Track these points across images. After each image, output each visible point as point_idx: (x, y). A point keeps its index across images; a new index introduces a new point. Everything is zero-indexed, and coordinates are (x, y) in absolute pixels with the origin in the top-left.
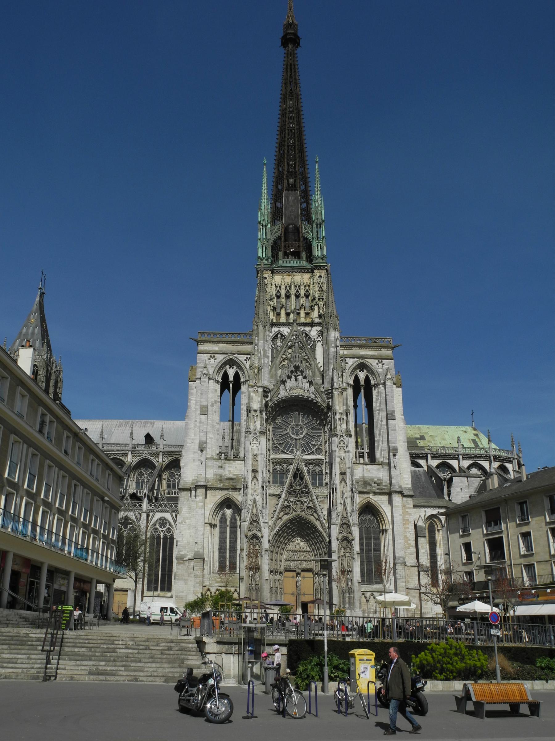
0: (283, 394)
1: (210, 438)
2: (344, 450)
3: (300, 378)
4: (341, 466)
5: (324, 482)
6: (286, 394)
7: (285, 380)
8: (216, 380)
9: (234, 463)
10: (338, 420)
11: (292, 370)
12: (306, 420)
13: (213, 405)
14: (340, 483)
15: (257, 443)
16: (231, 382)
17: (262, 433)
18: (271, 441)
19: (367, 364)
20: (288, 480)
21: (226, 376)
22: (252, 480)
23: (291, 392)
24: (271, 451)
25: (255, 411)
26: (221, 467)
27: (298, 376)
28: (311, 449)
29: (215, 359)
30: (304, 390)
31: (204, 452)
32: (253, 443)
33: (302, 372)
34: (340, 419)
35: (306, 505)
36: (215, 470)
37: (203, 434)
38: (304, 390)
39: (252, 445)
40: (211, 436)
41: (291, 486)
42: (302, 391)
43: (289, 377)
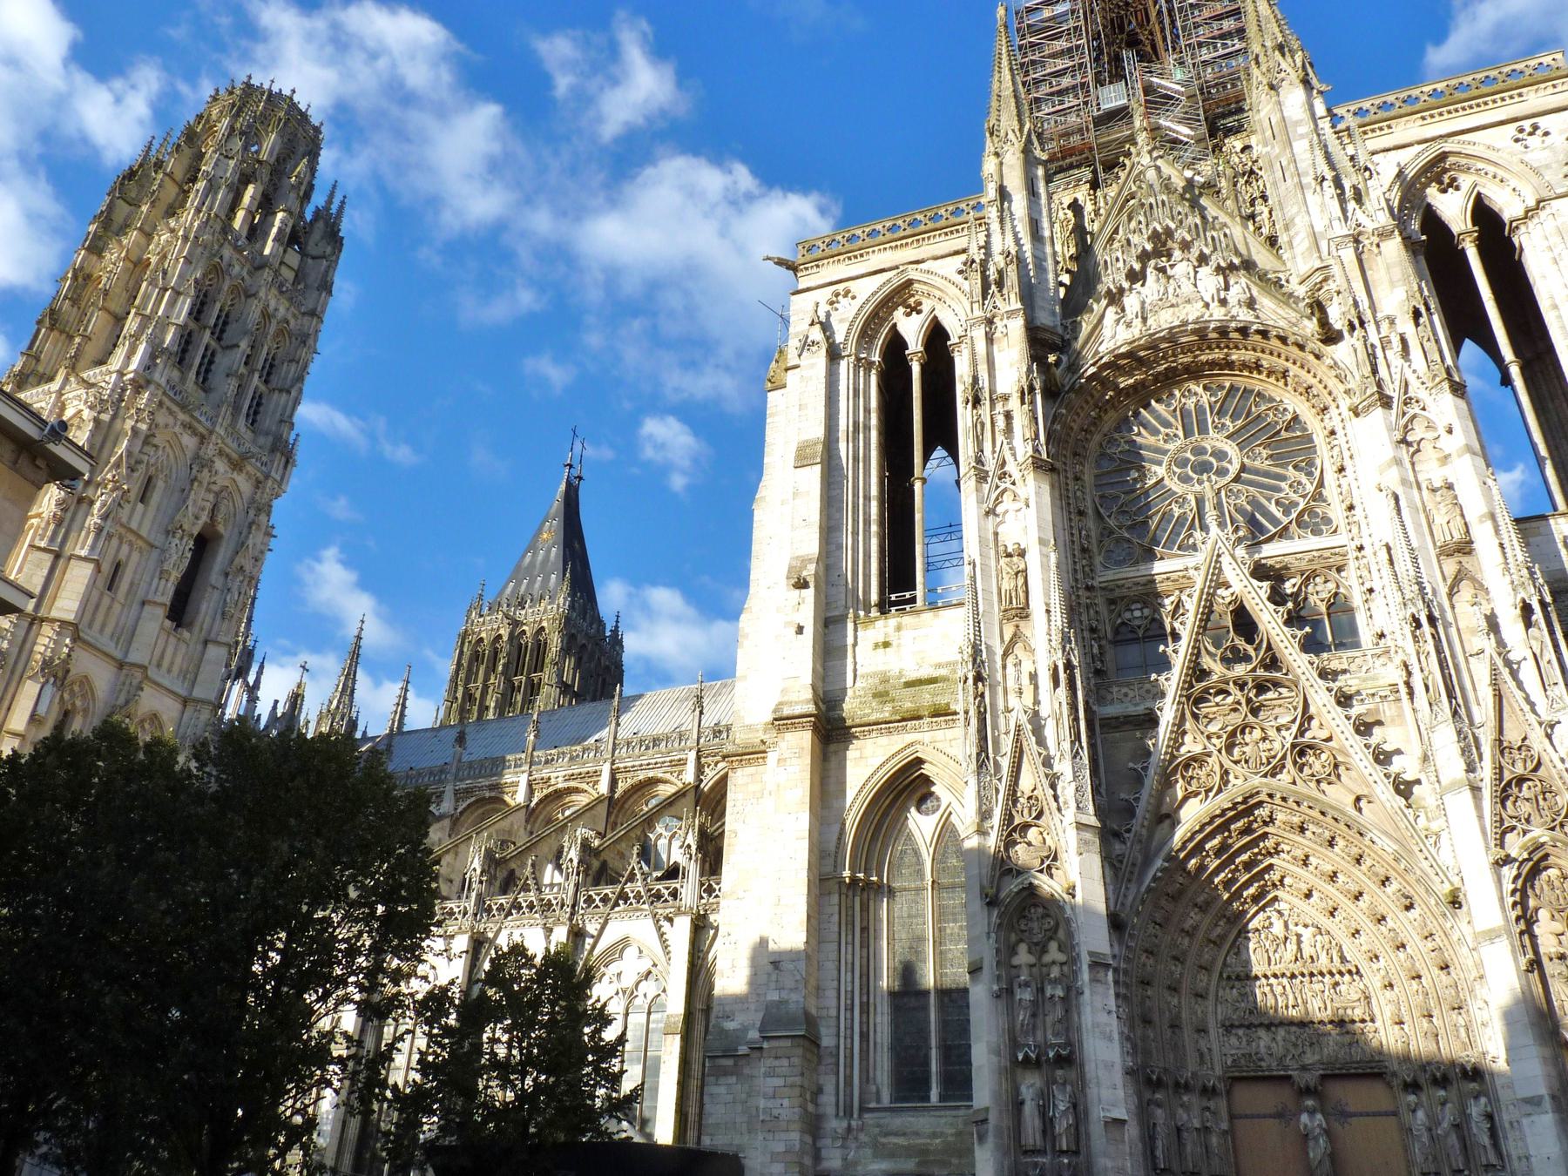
5: (1366, 635)
7: (1121, 291)
12: (1234, 418)
14: (1451, 595)
18: (1091, 523)
19: (1470, 150)
21: (896, 344)
24: (1098, 560)
26: (886, 645)
27: (1172, 266)
28: (1274, 521)
29: (854, 298)
30: (1207, 305)
33: (1186, 246)
38: (1207, 305)
41: (1197, 672)
43: (1135, 277)
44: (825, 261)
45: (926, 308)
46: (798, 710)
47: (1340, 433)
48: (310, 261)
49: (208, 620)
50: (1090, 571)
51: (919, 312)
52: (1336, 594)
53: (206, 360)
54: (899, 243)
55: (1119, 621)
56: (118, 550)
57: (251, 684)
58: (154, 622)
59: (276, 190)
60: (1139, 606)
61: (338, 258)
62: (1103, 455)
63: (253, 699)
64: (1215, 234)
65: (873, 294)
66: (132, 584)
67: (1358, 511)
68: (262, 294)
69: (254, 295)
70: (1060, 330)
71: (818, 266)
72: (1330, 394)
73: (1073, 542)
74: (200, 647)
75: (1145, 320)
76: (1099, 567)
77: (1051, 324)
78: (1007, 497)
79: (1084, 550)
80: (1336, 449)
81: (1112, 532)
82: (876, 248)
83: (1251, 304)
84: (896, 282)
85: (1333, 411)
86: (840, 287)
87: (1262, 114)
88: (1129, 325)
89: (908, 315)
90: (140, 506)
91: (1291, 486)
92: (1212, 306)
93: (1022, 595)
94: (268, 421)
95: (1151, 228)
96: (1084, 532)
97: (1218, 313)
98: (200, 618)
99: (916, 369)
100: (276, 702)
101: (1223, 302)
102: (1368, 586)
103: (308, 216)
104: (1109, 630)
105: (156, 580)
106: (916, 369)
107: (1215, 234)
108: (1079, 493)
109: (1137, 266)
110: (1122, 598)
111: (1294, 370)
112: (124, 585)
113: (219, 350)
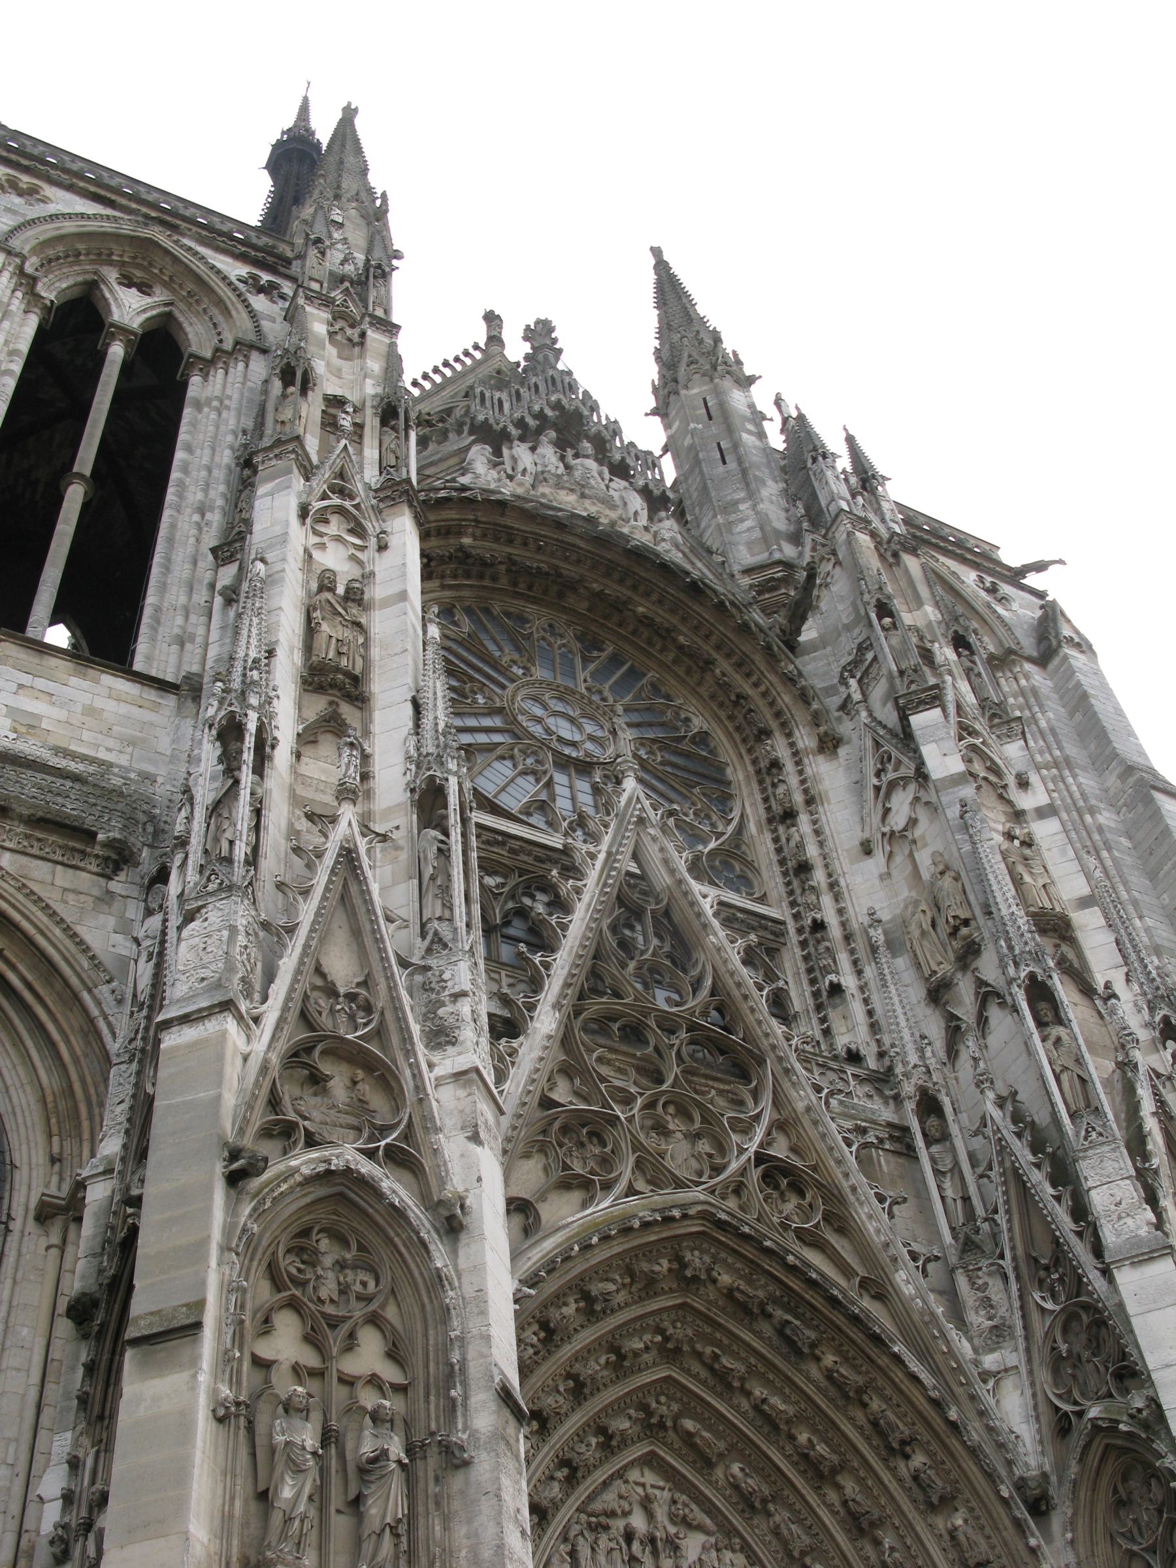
2: (1001, 807)
9: (74, 681)
16: (124, 330)
35: (753, 1147)
99: (117, 351)
106: (117, 351)
111: (723, 665)
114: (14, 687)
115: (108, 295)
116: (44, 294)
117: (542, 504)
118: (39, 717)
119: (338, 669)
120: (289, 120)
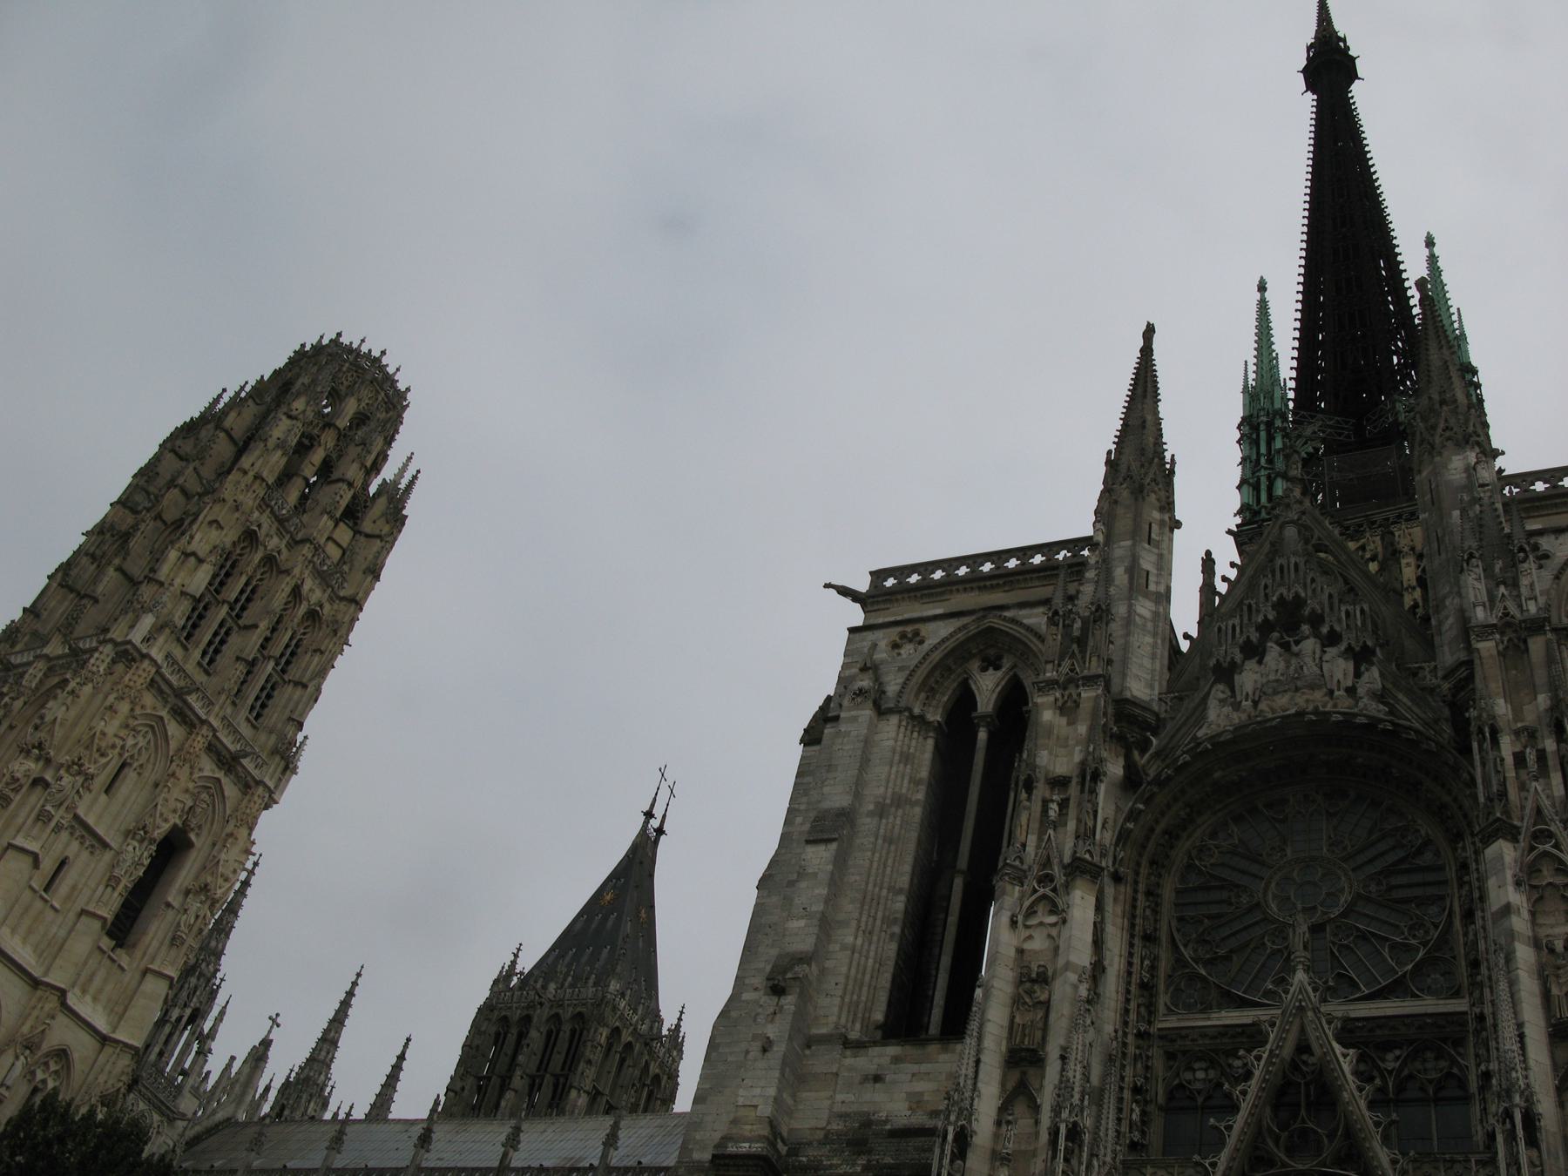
0: (1219, 717)
1: (844, 947)
3: (1309, 645)
4: (1555, 991)
6: (1237, 718)
8: (912, 717)
9: (943, 1057)
10: (1509, 760)
11: (1266, 620)
13: (881, 811)
15: (1052, 919)
16: (983, 717)
17: (1078, 868)
20: (1239, 1121)
22: (1004, 1108)
23: (1263, 706)
24: (1163, 1000)
25: (1060, 783)
27: (1297, 643)
30: (1331, 692)
31: (789, 1001)
32: (1033, 921)
33: (1316, 620)
34: (1520, 759)
36: (839, 1097)
37: (802, 923)
39: (1025, 933)
40: (850, 939)
42: (1318, 695)
43: (1254, 651)
44: (899, 597)
45: (1007, 663)
46: (745, 1147)
47: (1474, 866)
48: (362, 539)
49: (155, 944)
50: (1150, 1009)
51: (997, 668)
52: (1449, 1075)
53: (218, 638)
54: (988, 583)
55: (1176, 1082)
56: (67, 845)
57: (206, 1031)
58: (88, 937)
59: (340, 456)
60: (1204, 1065)
61: (395, 539)
62: (1190, 867)
63: (203, 1053)
64: (1350, 608)
65: (943, 641)
66: (74, 888)
67: (1484, 970)
68: (296, 571)
69: (287, 572)
70: (1156, 707)
71: (890, 601)
72: (1465, 816)
73: (1130, 974)
74: (137, 976)
75: (1255, 703)
76: (1162, 1009)
77: (1146, 698)
78: (1040, 908)
79: (1143, 986)
80: (1466, 888)
81: (1185, 965)
82: (961, 587)
83: (1381, 697)
84: (973, 629)
85: (1468, 840)
86: (909, 629)
87: (1424, 474)
88: (1237, 706)
89: (984, 669)
90: (103, 797)
91: (1411, 928)
92: (1337, 693)
93: (1039, 1034)
94: (274, 716)
95: (1277, 594)
96: (1147, 962)
97: (1345, 704)
98: (147, 939)
99: (982, 735)
100: (233, 1058)
101: (1351, 691)
102: (1483, 1067)
103: (373, 489)
104: (1161, 1092)
105: (101, 888)
106: (982, 735)
107: (1350, 608)
108: (1148, 912)
109: (1255, 637)
110: (1184, 1053)
112: (63, 887)
113: (235, 628)
114: (909, 1076)
115: (973, 687)
116: (932, 719)
117: (1259, 723)
118: (921, 1094)
119: (1022, 1050)
120: (1308, 33)
